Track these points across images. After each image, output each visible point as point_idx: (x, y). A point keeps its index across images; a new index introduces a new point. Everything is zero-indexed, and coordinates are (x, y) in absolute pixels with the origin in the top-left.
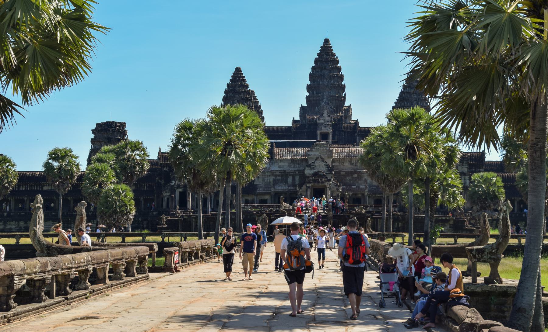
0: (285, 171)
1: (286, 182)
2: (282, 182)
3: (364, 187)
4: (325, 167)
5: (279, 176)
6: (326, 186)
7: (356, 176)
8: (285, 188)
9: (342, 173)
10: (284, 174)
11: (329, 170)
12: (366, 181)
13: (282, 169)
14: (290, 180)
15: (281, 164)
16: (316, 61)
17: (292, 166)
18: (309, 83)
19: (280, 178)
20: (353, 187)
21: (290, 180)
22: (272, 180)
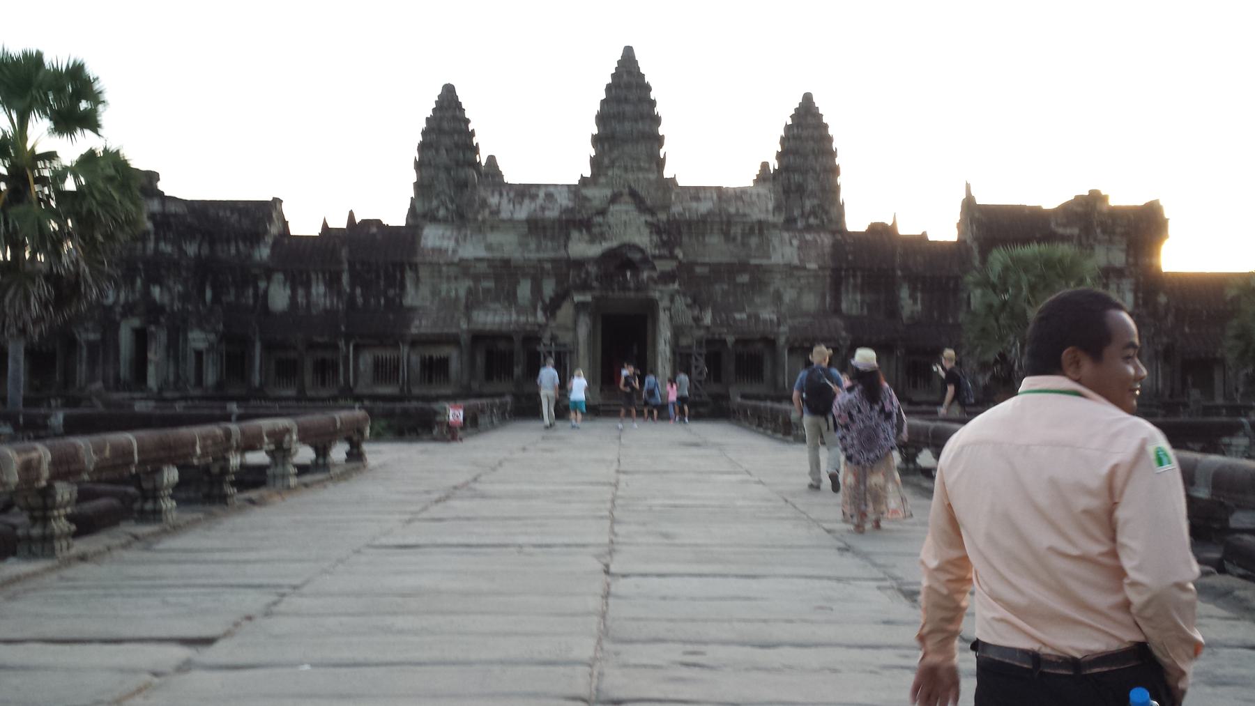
0: (506, 263)
1: (511, 297)
2: (497, 299)
3: (774, 317)
4: (646, 231)
5: (486, 276)
6: (650, 308)
7: (744, 278)
8: (506, 319)
9: (698, 270)
10: (504, 274)
11: (664, 244)
12: (778, 297)
13: (498, 255)
14: (524, 290)
15: (493, 238)
16: (609, 88)
17: (533, 246)
18: (596, 131)
19: (489, 284)
20: (738, 316)
21: (524, 290)
22: (462, 293)
